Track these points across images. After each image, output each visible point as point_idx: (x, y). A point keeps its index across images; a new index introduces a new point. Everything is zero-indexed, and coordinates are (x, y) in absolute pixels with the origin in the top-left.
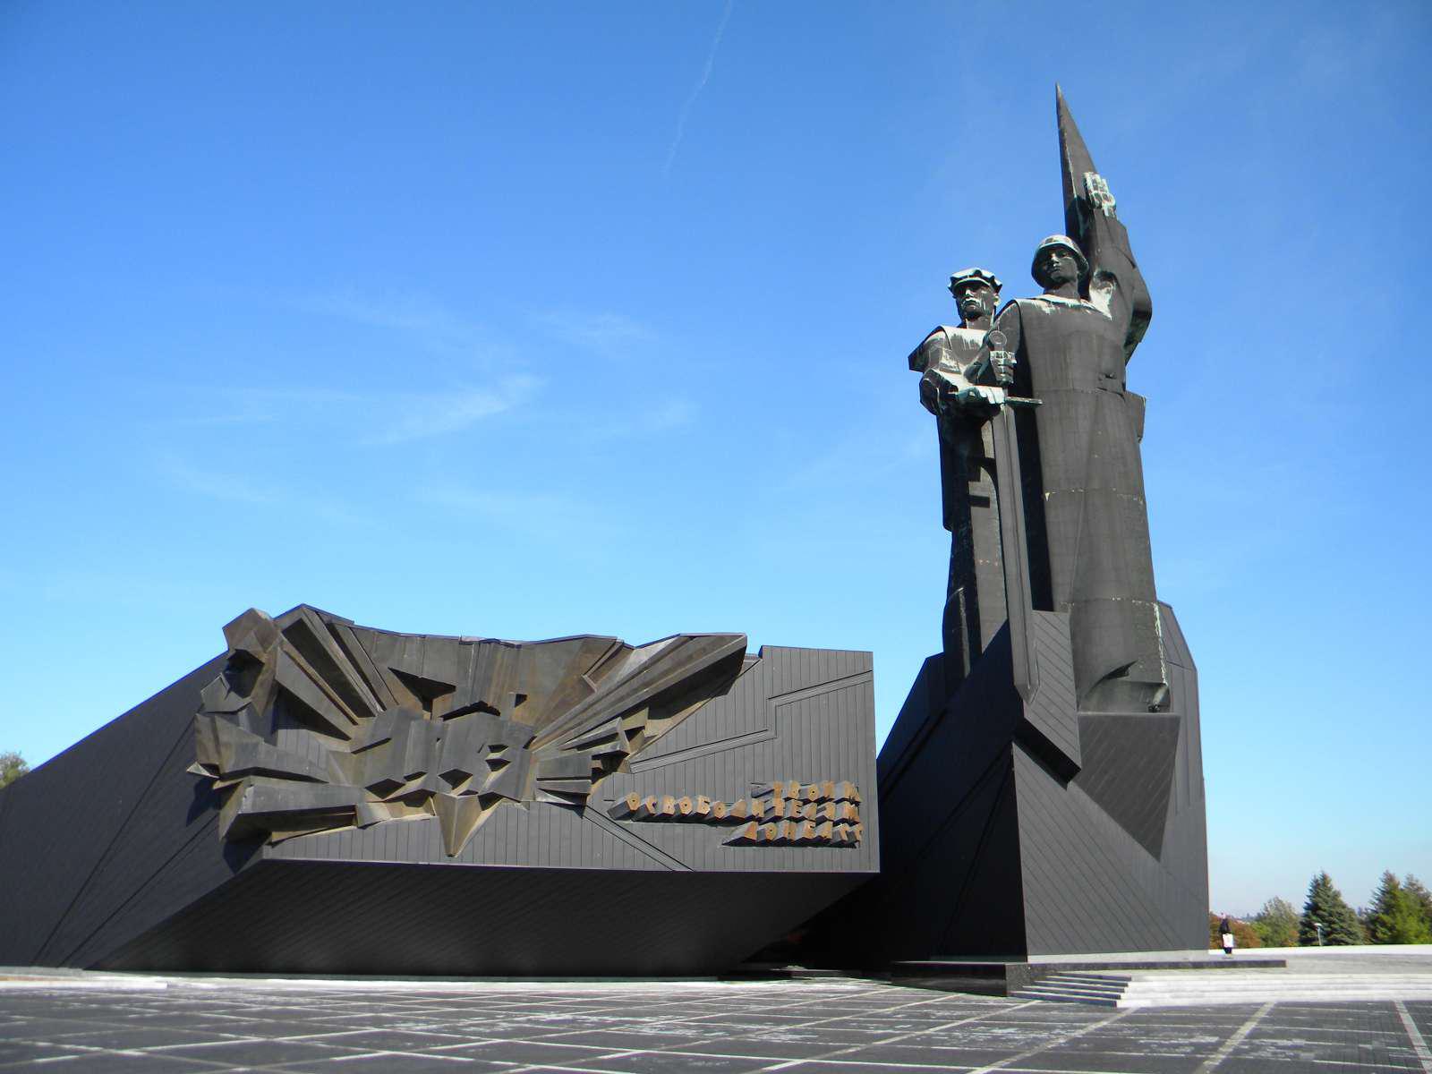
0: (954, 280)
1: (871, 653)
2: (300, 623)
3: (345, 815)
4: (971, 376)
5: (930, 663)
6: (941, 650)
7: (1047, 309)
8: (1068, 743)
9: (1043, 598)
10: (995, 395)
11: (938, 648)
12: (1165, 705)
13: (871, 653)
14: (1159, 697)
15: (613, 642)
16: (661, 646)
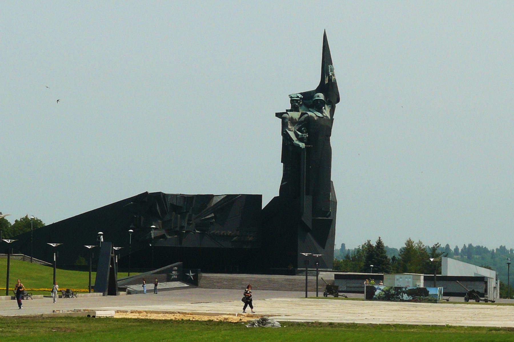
0: (291, 97)
1: (261, 195)
2: (160, 196)
3: (163, 236)
4: (297, 135)
5: (275, 198)
6: (278, 195)
7: (316, 118)
8: (309, 224)
9: (308, 194)
10: (302, 145)
11: (278, 195)
12: (330, 215)
13: (261, 195)
14: (329, 213)
15: (212, 195)
16: (223, 197)
